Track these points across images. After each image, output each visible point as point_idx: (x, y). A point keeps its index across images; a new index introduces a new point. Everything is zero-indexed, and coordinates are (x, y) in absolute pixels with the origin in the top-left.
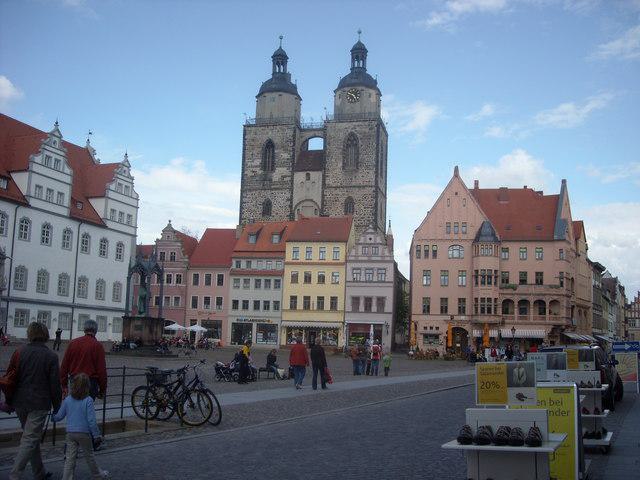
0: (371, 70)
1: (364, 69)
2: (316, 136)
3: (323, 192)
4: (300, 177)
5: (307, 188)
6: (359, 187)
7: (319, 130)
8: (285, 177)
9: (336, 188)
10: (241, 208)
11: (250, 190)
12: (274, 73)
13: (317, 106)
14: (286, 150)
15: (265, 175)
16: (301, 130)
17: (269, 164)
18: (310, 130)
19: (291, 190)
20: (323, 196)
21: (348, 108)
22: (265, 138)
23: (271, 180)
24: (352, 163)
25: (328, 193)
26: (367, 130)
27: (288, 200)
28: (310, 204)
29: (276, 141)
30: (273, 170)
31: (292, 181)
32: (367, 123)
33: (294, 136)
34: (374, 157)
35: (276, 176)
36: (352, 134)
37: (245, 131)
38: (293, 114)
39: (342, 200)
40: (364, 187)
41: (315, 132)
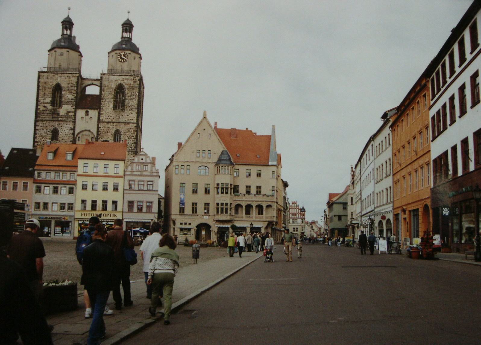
0: (135, 40)
1: (130, 39)
2: (92, 84)
3: (98, 125)
4: (81, 113)
5: (86, 121)
7: (97, 80)
8: (70, 112)
9: (108, 123)
11: (42, 121)
12: (63, 34)
13: (95, 62)
14: (71, 93)
16: (83, 79)
17: (57, 102)
19: (74, 122)
20: (98, 128)
21: (119, 66)
22: (55, 83)
23: (58, 114)
24: (119, 104)
26: (132, 83)
27: (71, 129)
28: (87, 133)
29: (64, 85)
30: (60, 106)
31: (75, 116)
32: (132, 78)
34: (136, 102)
35: (63, 111)
37: (39, 76)
39: (113, 131)
40: (128, 123)
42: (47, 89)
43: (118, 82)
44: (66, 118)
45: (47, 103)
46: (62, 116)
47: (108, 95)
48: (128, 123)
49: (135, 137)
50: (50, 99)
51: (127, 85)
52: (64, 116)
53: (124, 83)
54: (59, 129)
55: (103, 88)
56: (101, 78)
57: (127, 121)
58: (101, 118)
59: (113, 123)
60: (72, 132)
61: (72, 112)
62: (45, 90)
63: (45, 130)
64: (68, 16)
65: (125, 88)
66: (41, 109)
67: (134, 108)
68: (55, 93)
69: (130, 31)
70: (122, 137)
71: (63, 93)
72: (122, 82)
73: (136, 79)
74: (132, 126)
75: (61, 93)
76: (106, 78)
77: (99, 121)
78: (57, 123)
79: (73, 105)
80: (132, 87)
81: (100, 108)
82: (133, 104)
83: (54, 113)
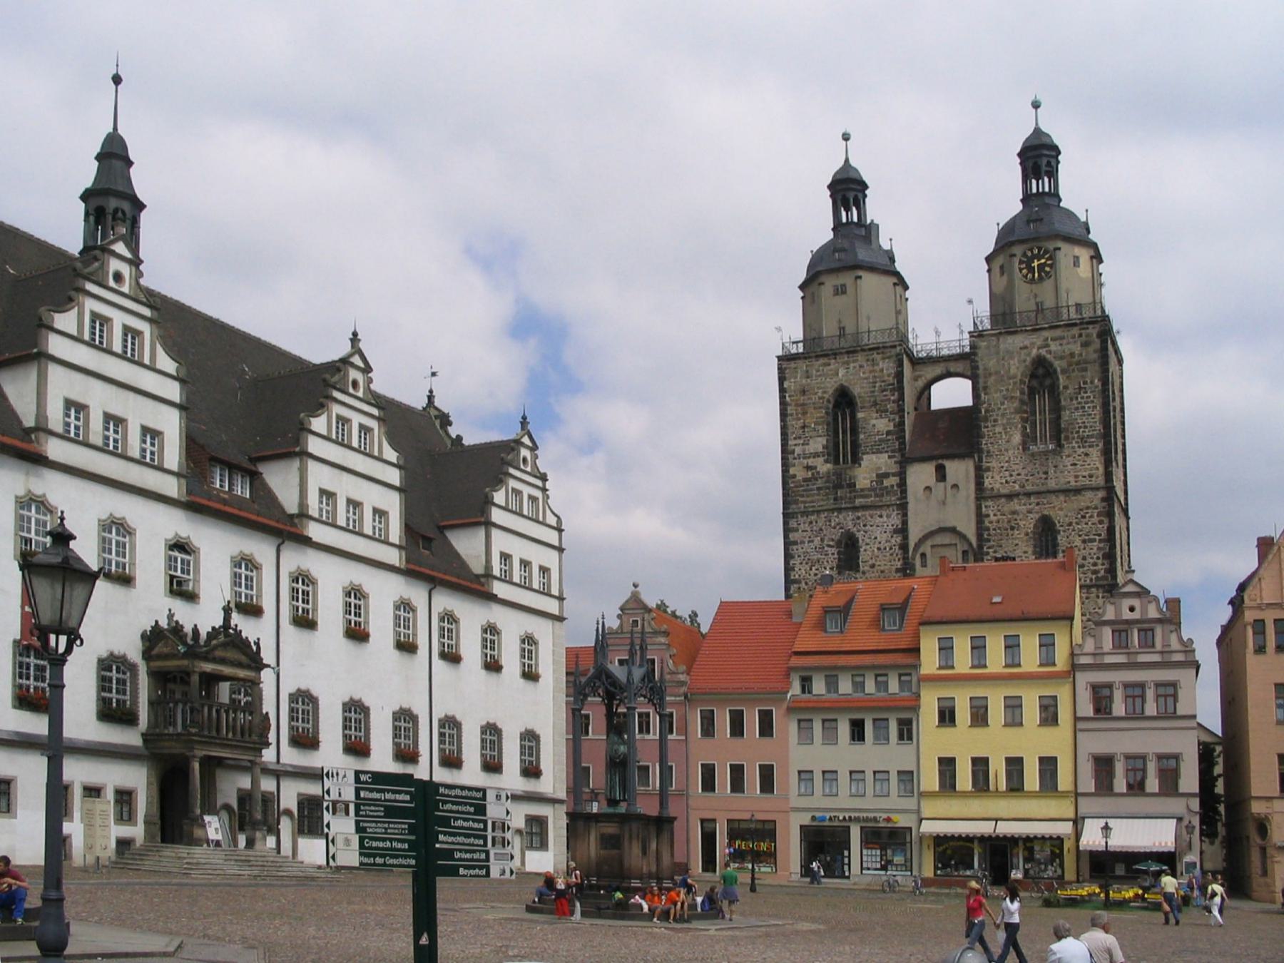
2: (949, 375)
3: (979, 508)
4: (920, 475)
5: (940, 499)
6: (1066, 492)
8: (886, 475)
9: (1010, 497)
10: (788, 556)
11: (805, 513)
14: (882, 412)
15: (839, 475)
16: (916, 362)
17: (845, 448)
18: (930, 360)
19: (903, 507)
20: (980, 517)
22: (831, 386)
23: (852, 486)
26: (1077, 348)
27: (896, 531)
28: (946, 539)
29: (858, 390)
30: (856, 460)
31: (903, 484)
32: (1075, 331)
33: (899, 375)
34: (1098, 411)
35: (863, 476)
36: (1040, 362)
37: (781, 370)
38: (892, 323)
39: (1028, 524)
40: (1077, 491)
41: (948, 365)
43: (1029, 354)
44: (876, 496)
45: (816, 455)
46: (862, 490)
47: (1003, 404)
48: (1077, 491)
49: (1104, 535)
50: (823, 441)
51: (1062, 358)
52: (869, 490)
53: (1050, 352)
54: (860, 535)
55: (981, 381)
56: (973, 346)
57: (1073, 483)
58: (987, 482)
59: (1028, 495)
60: (898, 539)
61: (894, 475)
62: (805, 413)
63: (817, 541)
64: (847, 160)
65: (1055, 371)
66: (799, 478)
67: (1092, 436)
68: (836, 420)
69: (1053, 174)
70: (1062, 539)
71: (860, 415)
72: (1043, 352)
73: (1087, 335)
75: (853, 416)
76: (988, 347)
77: (981, 493)
78: (851, 515)
79: (893, 451)
80: (1078, 363)
81: (980, 451)
82: (1089, 421)
83: (838, 486)
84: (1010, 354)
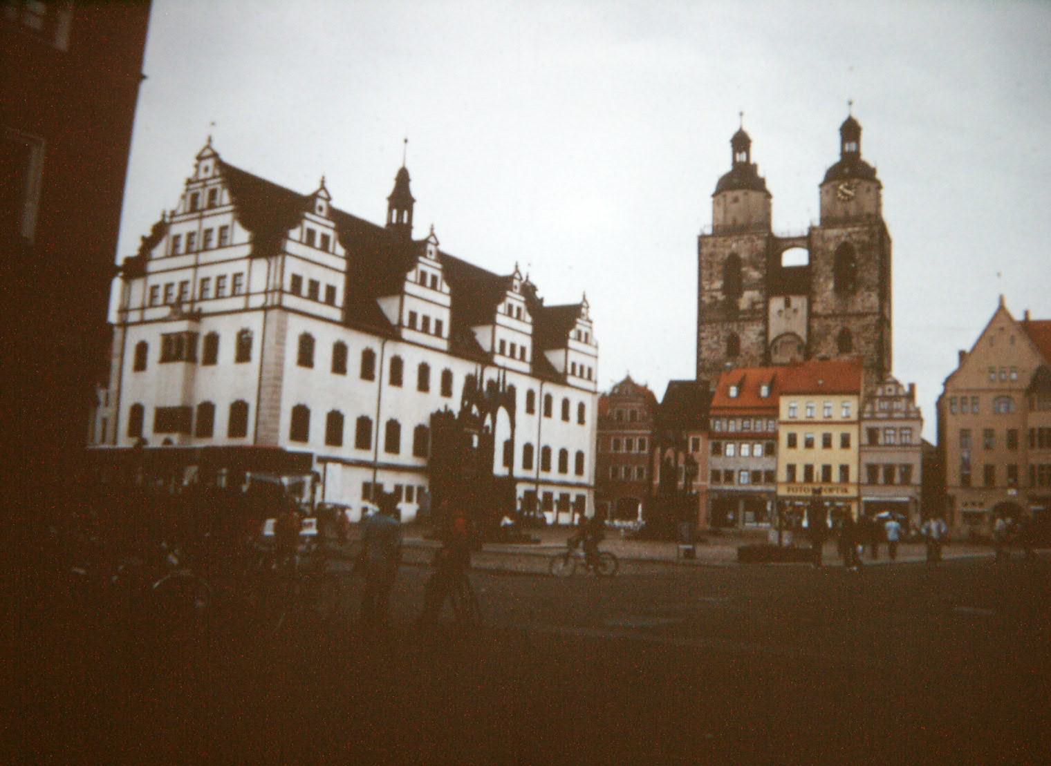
1: (857, 154)
4: (776, 304)
5: (786, 317)
9: (826, 317)
10: (699, 346)
12: (735, 163)
13: (795, 208)
14: (756, 268)
17: (734, 286)
20: (809, 328)
22: (727, 252)
23: (737, 308)
24: (847, 283)
25: (816, 325)
26: (866, 238)
29: (743, 255)
31: (766, 309)
36: (845, 244)
39: (836, 332)
41: (791, 242)
42: (715, 265)
45: (717, 290)
60: (761, 339)
74: (871, 320)
84: (829, 240)
